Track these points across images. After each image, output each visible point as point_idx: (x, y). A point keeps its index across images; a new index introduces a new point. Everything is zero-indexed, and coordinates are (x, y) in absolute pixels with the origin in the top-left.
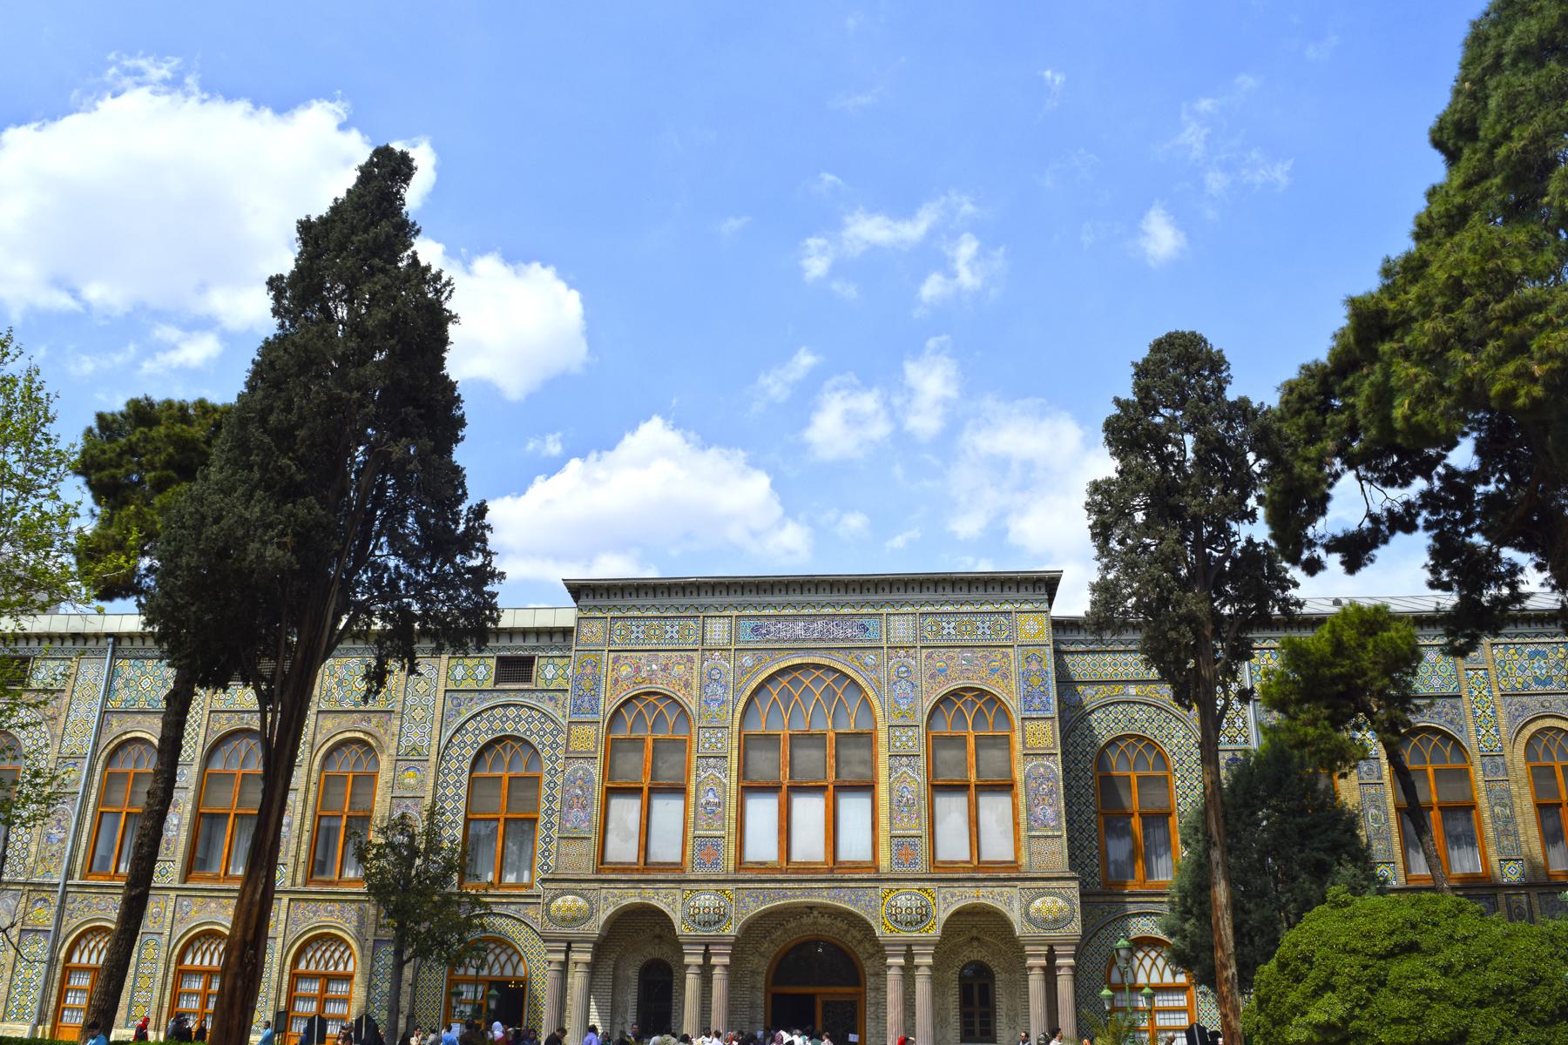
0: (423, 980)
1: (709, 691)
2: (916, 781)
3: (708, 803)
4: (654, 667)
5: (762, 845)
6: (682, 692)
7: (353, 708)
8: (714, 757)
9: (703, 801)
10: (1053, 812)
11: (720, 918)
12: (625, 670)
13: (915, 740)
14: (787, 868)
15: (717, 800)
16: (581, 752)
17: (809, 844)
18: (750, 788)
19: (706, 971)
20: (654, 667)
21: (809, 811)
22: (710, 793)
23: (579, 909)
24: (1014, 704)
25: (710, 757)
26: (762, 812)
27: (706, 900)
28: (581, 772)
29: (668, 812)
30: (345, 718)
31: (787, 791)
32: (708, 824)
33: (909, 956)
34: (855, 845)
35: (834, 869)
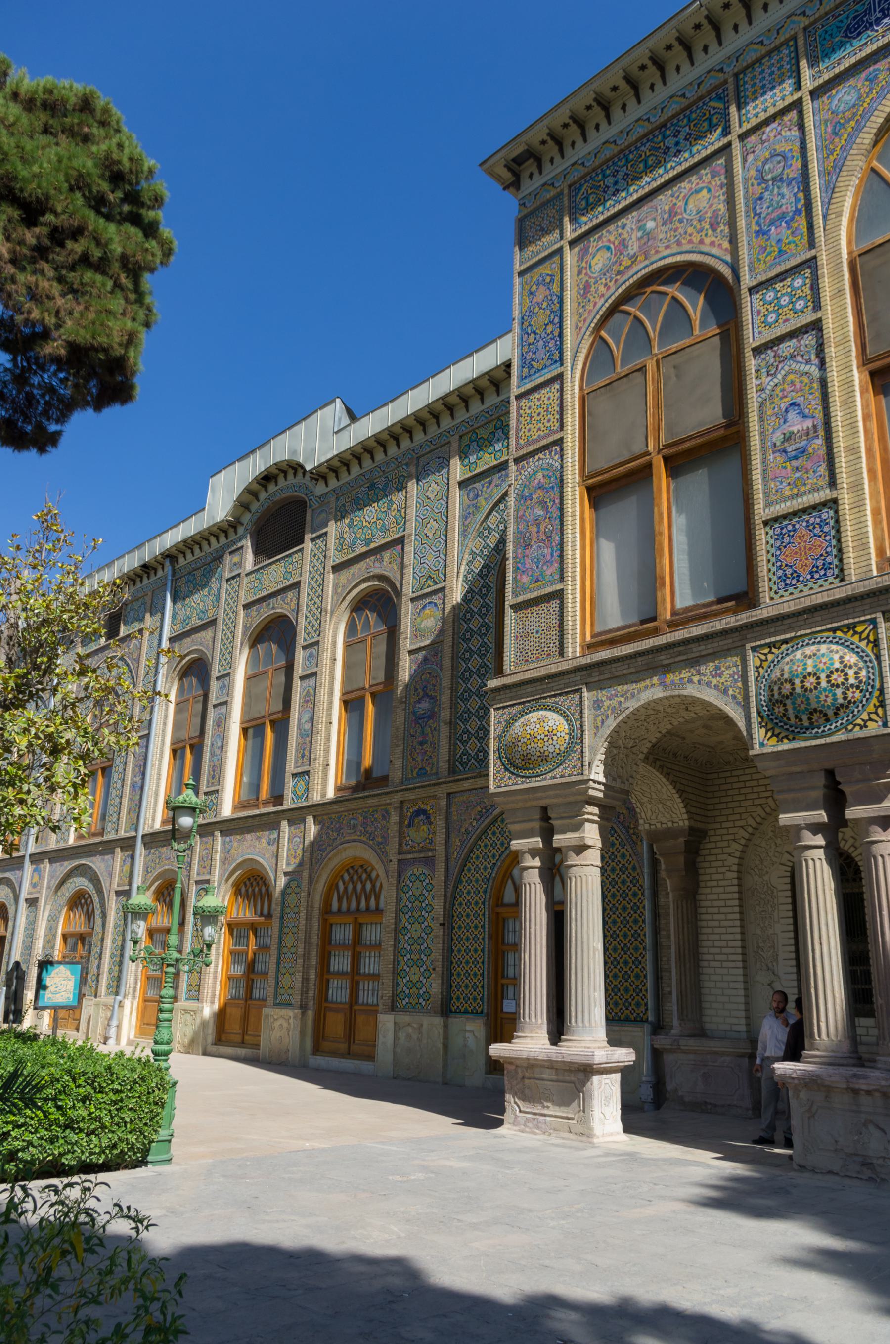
0: (460, 916)
1: (763, 208)
3: (788, 438)
4: (650, 225)
6: (707, 241)
7: (365, 549)
8: (792, 335)
9: (778, 437)
12: (599, 261)
15: (809, 423)
16: (540, 438)
20: (650, 225)
22: (792, 415)
23: (551, 734)
25: (781, 339)
28: (540, 476)
30: (355, 569)
32: (792, 484)
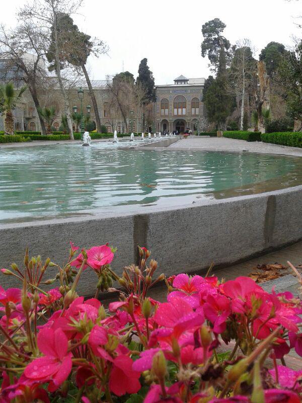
2: (190, 107)
5: (176, 113)
10: (202, 110)
11: (172, 120)
13: (190, 103)
14: (178, 115)
17: (180, 113)
18: (175, 108)
19: (171, 125)
21: (180, 110)
24: (200, 99)
26: (176, 110)
27: (171, 119)
29: (167, 110)
31: (178, 108)
33: (189, 123)
34: (184, 113)
35: (182, 116)
